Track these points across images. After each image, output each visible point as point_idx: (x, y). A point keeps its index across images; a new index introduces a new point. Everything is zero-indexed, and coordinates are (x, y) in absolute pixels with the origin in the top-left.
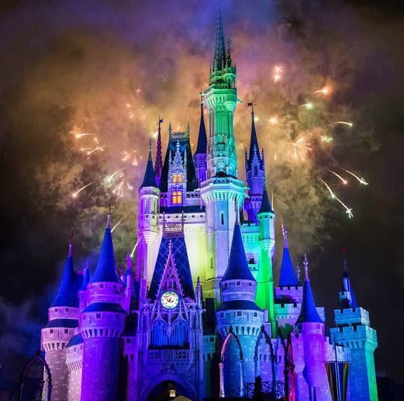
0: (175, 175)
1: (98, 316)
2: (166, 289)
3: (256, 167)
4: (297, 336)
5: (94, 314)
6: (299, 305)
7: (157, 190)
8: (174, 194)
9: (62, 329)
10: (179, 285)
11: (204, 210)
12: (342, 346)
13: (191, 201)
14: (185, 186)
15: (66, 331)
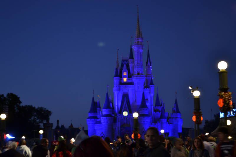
0: (124, 73)
1: (107, 118)
2: (124, 111)
3: (149, 65)
4: (159, 122)
5: (105, 118)
6: (160, 112)
7: (119, 78)
8: (124, 78)
9: (93, 119)
10: (128, 110)
11: (133, 84)
12: (172, 124)
13: (130, 81)
14: (127, 76)
15: (94, 120)
